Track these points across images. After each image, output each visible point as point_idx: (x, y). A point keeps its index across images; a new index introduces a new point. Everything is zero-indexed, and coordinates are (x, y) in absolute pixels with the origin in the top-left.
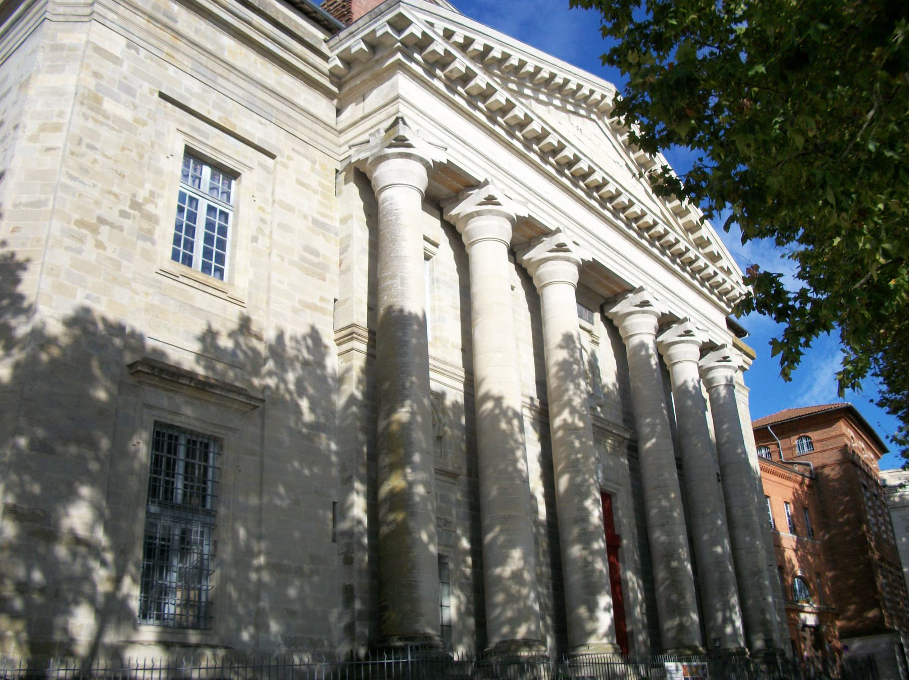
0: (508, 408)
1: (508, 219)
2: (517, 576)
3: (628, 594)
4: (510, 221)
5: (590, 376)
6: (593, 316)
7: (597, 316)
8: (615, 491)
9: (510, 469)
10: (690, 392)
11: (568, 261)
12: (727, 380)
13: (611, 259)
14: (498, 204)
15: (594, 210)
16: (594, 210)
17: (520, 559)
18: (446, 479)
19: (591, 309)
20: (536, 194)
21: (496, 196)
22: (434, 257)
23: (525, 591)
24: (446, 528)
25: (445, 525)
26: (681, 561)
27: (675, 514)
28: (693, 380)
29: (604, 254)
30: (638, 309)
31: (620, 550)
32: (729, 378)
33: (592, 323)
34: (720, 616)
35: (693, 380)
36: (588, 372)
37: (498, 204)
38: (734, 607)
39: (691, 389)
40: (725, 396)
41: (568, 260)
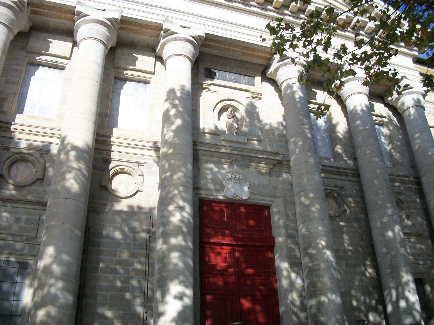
0: (68, 143)
1: (98, 23)
2: (47, 270)
3: (280, 282)
4: (101, 24)
5: (248, 120)
6: (254, 79)
7: (258, 79)
8: (271, 203)
9: (59, 188)
10: (359, 114)
11: (176, 40)
12: (415, 101)
13: (241, 33)
14: (86, 15)
15: (221, 5)
16: (221, 5)
17: (51, 256)
18: (36, 207)
19: (251, 75)
20: (143, 4)
21: (81, 10)
22: (66, 66)
23: (52, 281)
24: (28, 242)
25: (27, 240)
26: (320, 251)
27: (314, 209)
28: (360, 105)
29: (232, 31)
30: (281, 63)
31: (275, 248)
32: (416, 100)
33: (253, 85)
34: (394, 293)
35: (360, 105)
36: (245, 117)
37: (86, 15)
38: (407, 284)
39: (359, 111)
40: (414, 113)
41: (176, 39)
